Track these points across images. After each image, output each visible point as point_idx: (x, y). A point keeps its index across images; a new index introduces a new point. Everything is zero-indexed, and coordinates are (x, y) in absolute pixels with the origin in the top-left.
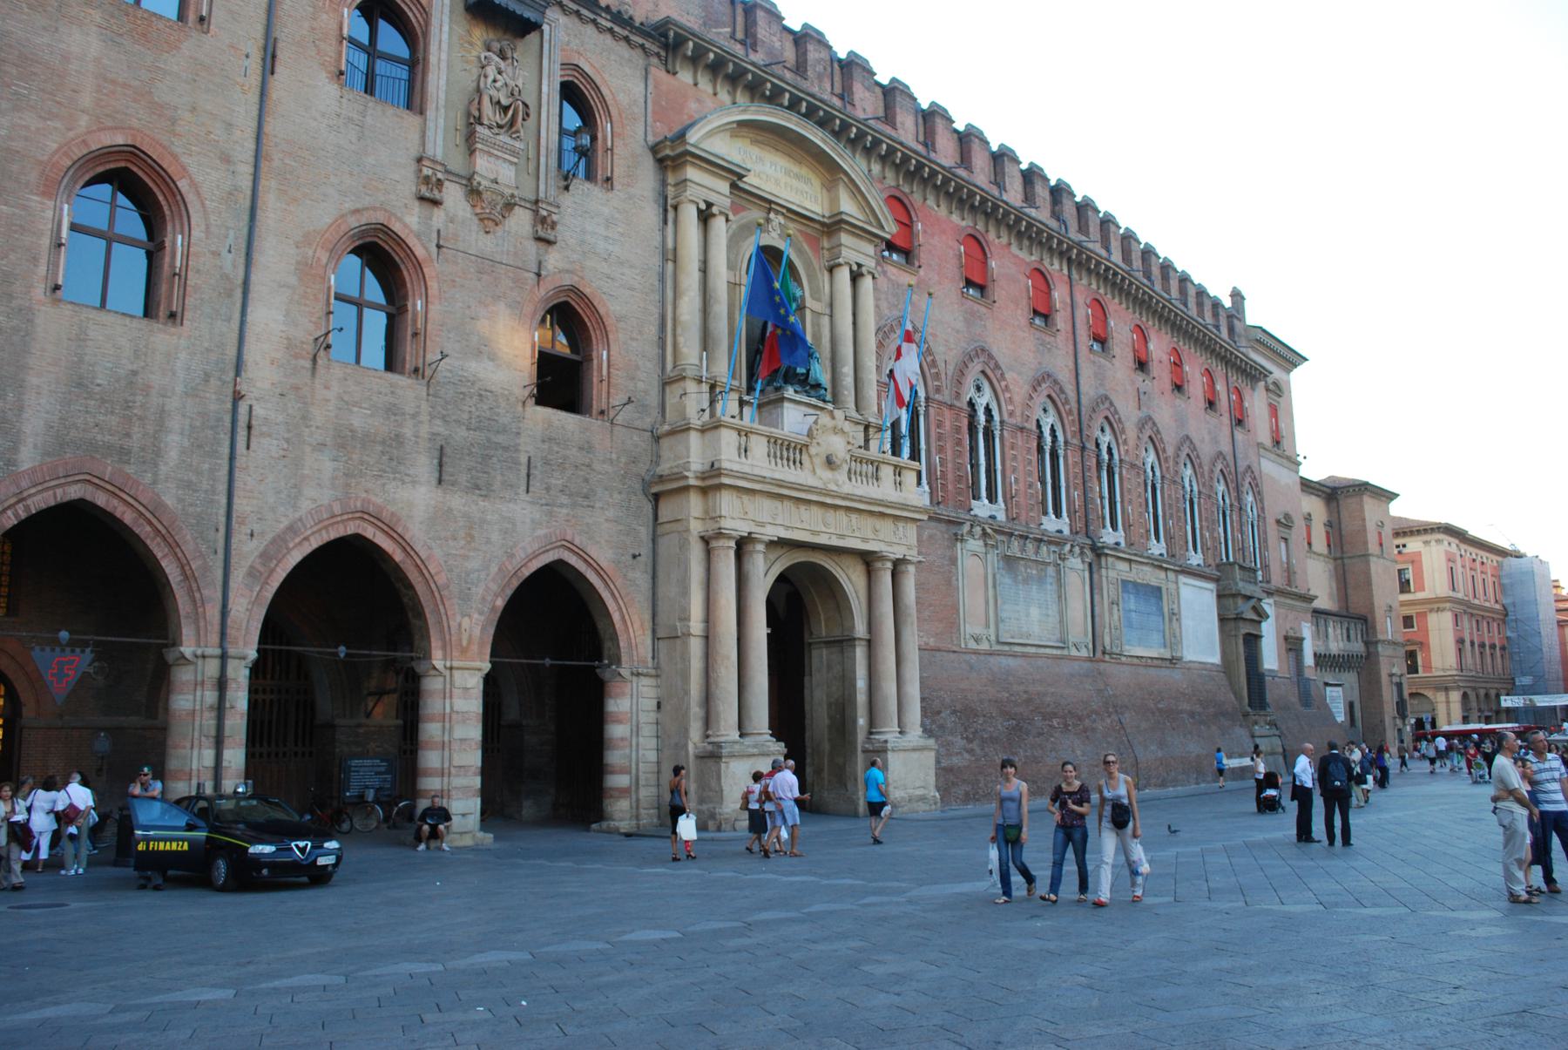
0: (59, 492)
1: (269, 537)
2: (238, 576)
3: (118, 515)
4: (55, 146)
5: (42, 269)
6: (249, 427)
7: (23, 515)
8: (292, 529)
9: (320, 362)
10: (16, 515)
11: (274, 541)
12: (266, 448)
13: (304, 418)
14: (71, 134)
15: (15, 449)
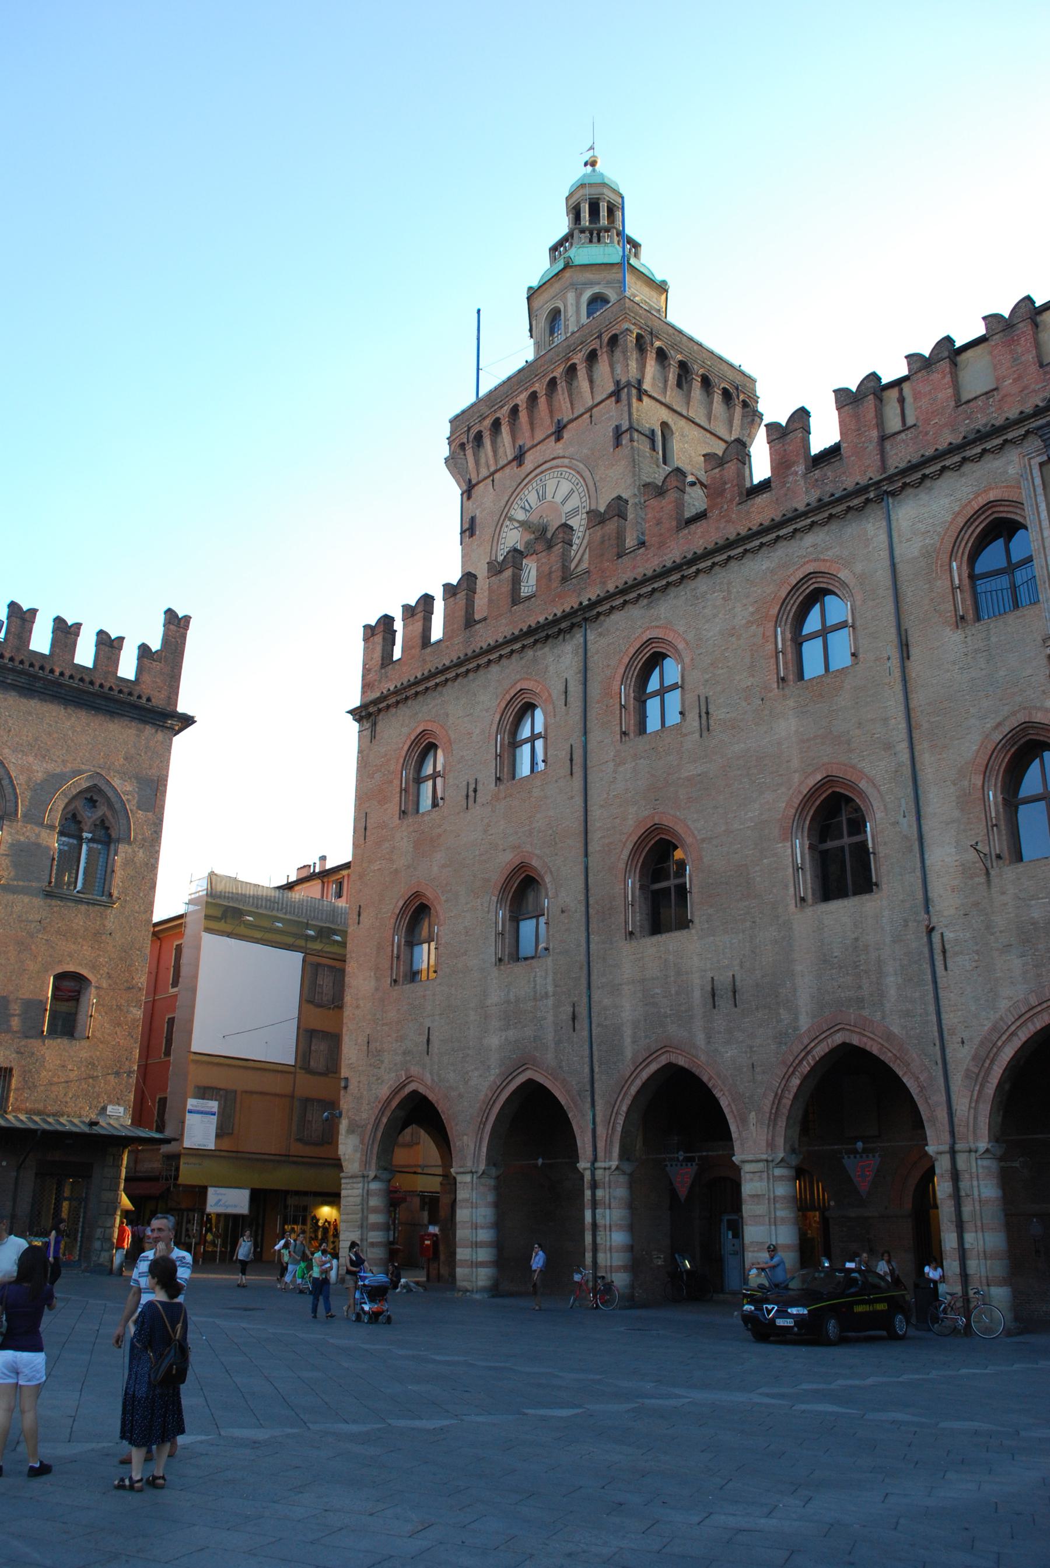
0: (829, 1040)
1: (977, 1041)
2: (957, 1081)
3: (868, 1048)
4: (784, 805)
5: (792, 890)
6: (944, 952)
7: (812, 1063)
8: (994, 1028)
9: (992, 872)
10: (809, 1063)
11: (982, 1043)
12: (960, 963)
13: (988, 927)
14: (791, 791)
15: (796, 1019)
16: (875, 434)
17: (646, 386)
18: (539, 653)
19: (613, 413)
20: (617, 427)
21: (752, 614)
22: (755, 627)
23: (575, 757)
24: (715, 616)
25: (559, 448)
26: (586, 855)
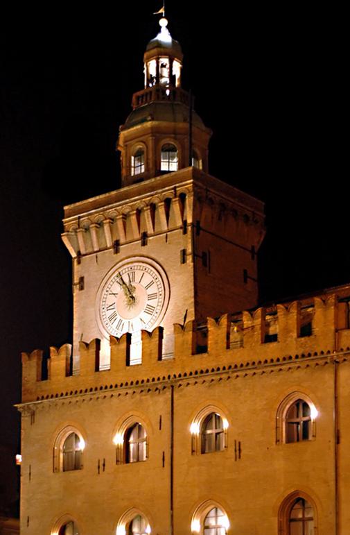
4: (275, 500)
16: (333, 328)
17: (201, 225)
18: (144, 397)
19: (181, 241)
20: (184, 252)
21: (265, 405)
22: (266, 412)
23: (166, 458)
24: (245, 401)
25: (144, 250)
26: (172, 509)
